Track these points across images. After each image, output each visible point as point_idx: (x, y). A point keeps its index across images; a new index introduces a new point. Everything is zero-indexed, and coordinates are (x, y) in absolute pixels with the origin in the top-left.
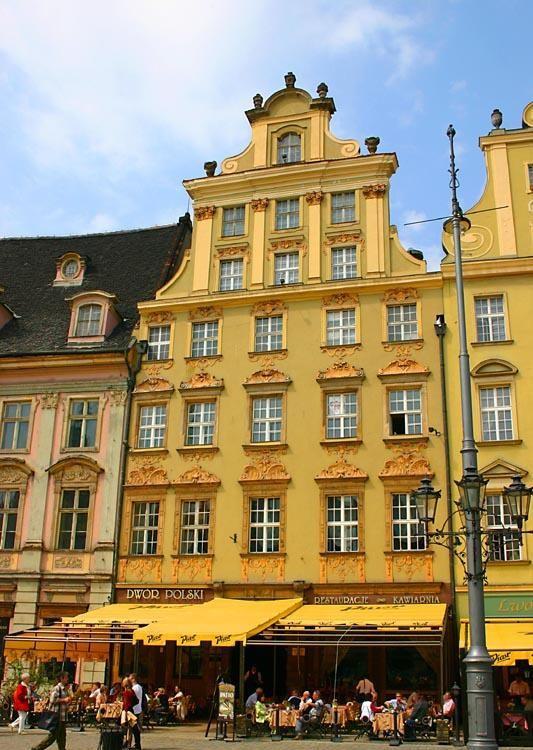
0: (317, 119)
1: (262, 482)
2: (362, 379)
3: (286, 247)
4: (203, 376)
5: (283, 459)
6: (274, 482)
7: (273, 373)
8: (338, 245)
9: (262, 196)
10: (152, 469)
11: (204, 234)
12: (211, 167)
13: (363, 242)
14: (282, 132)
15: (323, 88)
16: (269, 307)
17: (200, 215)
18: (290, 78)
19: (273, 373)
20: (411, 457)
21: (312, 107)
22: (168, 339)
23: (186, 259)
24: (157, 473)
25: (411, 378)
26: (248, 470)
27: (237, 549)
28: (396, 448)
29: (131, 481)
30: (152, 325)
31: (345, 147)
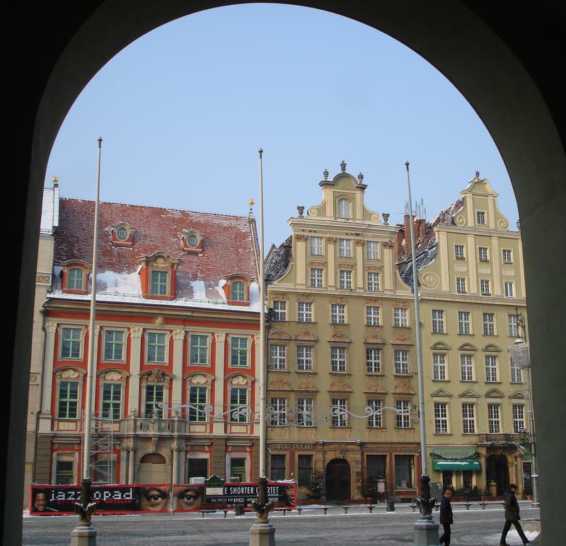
0: (358, 193)
1: (339, 392)
2: (384, 344)
3: (345, 268)
4: (307, 333)
5: (347, 380)
6: (344, 392)
7: (342, 336)
8: (371, 271)
9: (334, 236)
10: (282, 381)
11: (299, 249)
12: (301, 209)
13: (383, 272)
14: (341, 197)
15: (361, 177)
16: (338, 301)
17: (299, 238)
18: (343, 166)
19: (342, 336)
20: (405, 385)
21: (357, 187)
22: (285, 309)
23: (291, 264)
24: (285, 383)
25: (403, 347)
26: (332, 385)
27: (329, 424)
28: (399, 379)
29: (271, 388)
30: (275, 300)
31: (373, 216)
